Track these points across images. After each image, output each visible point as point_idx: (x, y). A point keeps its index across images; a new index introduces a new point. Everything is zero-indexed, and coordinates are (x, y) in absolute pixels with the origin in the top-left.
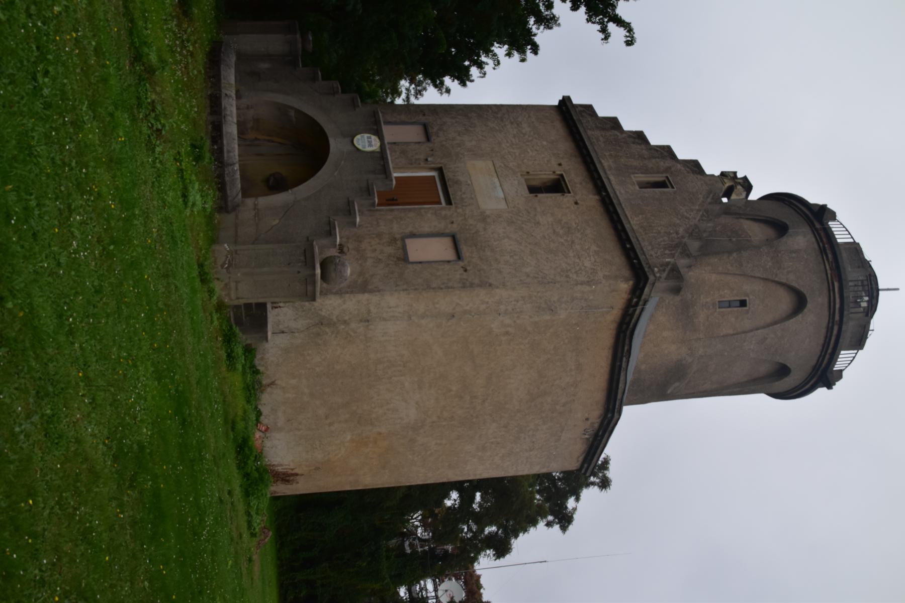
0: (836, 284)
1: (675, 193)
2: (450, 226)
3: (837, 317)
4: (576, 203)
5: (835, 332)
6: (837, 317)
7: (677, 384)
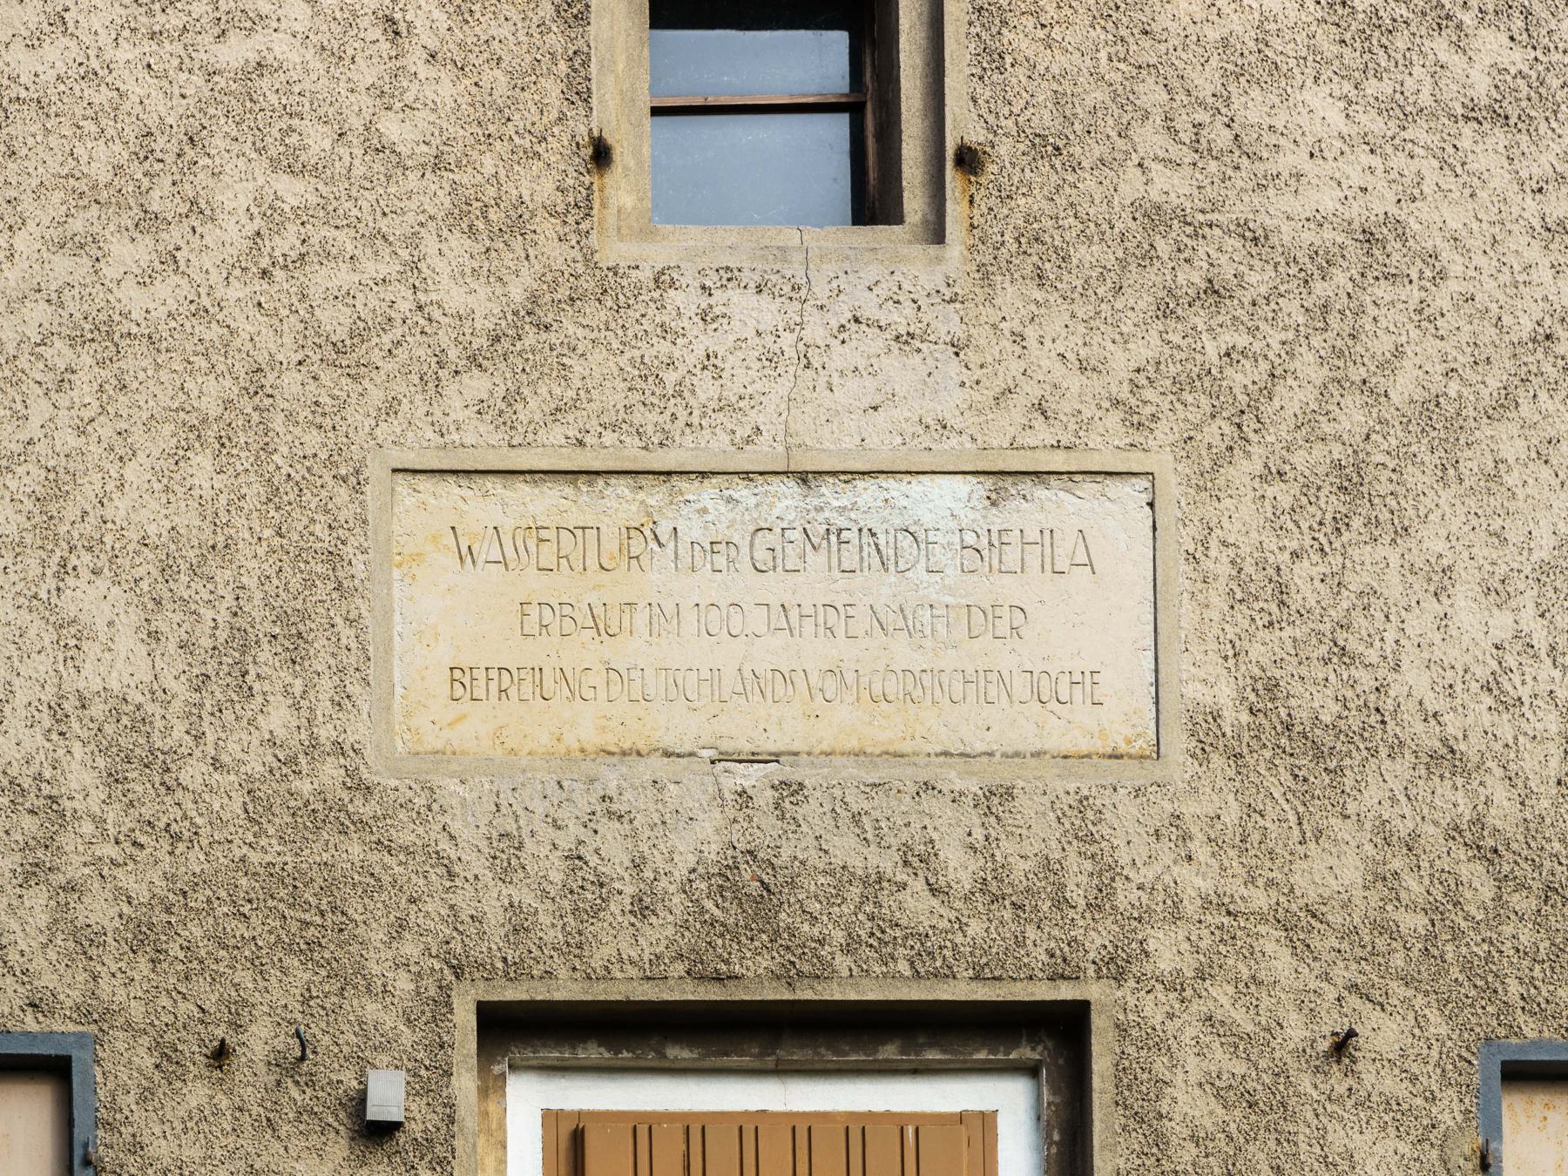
2: (1378, 1081)
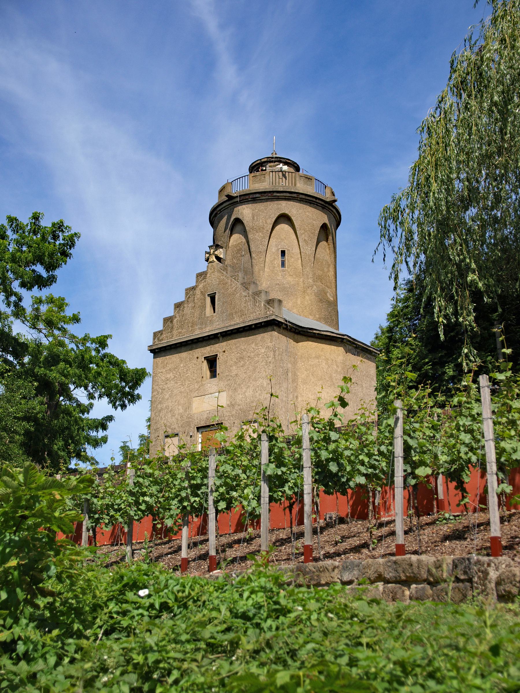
0: (275, 194)
1: (219, 293)
2: (236, 424)
3: (295, 195)
4: (224, 352)
5: (303, 197)
6: (295, 195)
7: (328, 295)
